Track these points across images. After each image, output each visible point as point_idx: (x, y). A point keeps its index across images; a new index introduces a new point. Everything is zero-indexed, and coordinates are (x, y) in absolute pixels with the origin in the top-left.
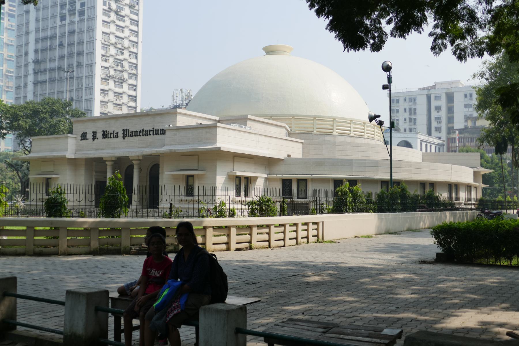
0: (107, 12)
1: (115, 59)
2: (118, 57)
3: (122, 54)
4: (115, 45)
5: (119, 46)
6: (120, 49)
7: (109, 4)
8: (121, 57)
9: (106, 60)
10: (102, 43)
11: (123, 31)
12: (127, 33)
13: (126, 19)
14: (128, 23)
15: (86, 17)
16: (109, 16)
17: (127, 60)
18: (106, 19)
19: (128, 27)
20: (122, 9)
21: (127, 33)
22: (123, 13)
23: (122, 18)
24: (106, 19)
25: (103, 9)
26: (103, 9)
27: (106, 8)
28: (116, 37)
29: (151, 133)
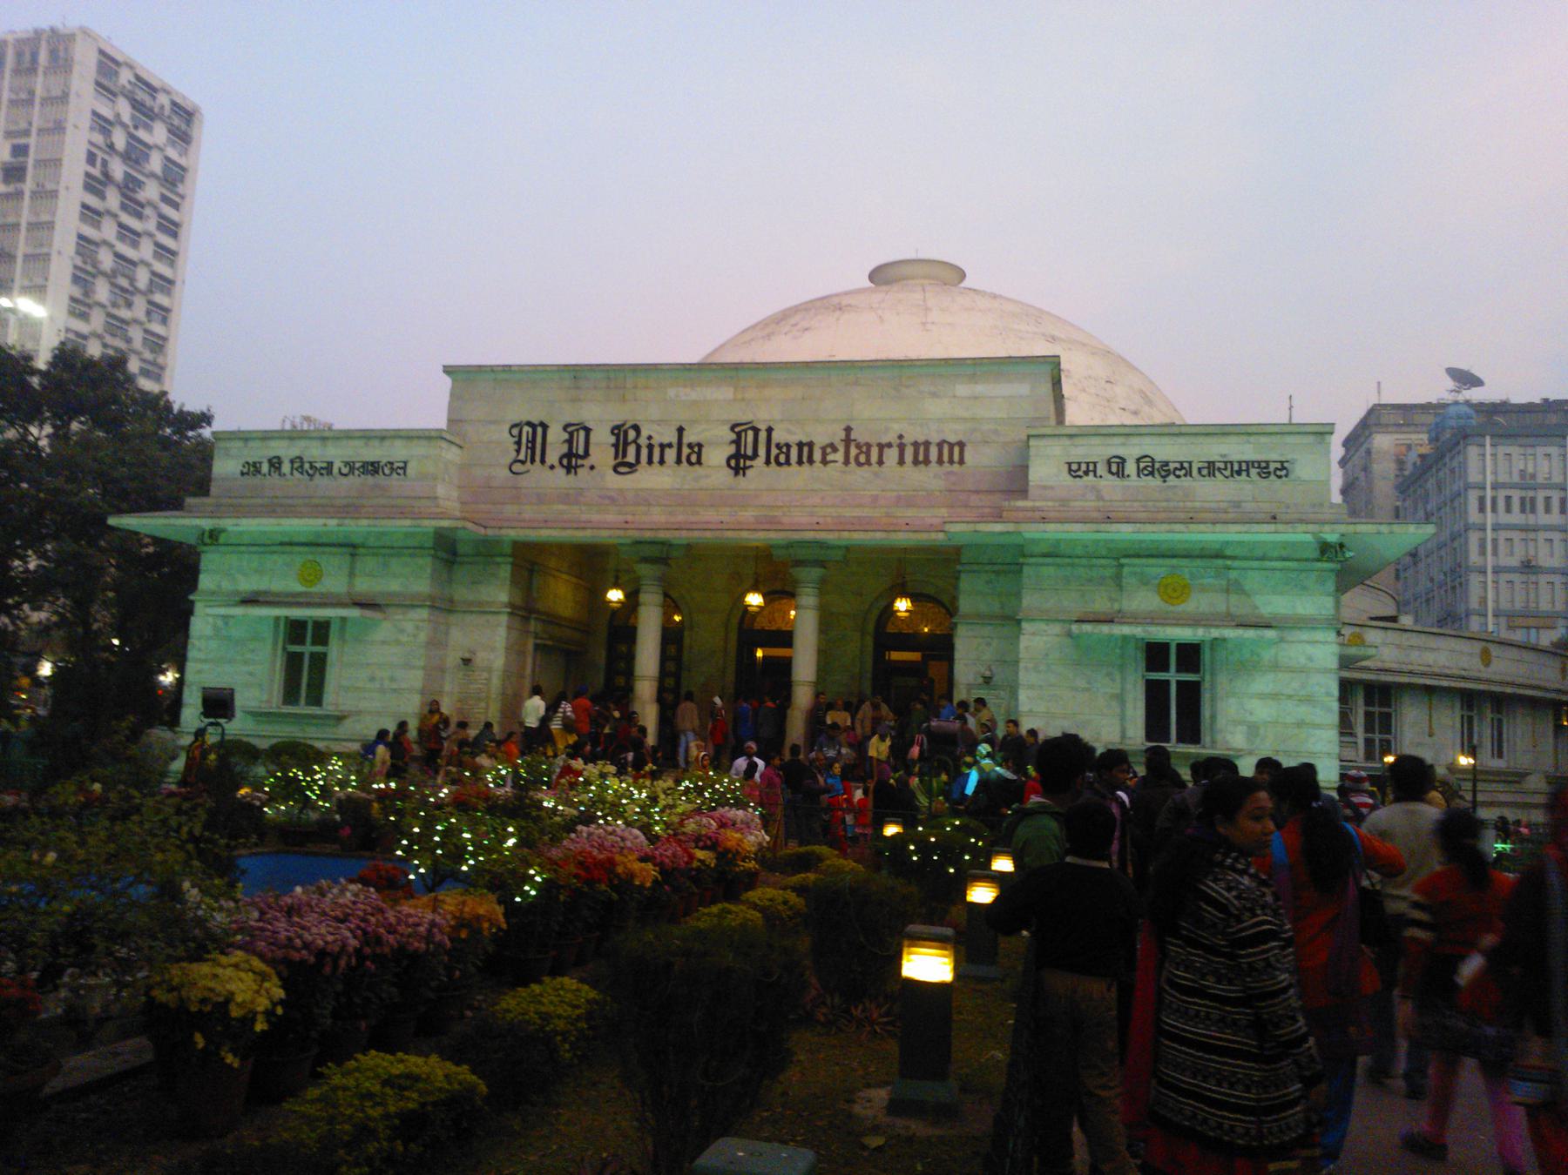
0: (95, 185)
1: (109, 315)
2: (115, 311)
3: (129, 305)
4: (110, 276)
5: (124, 282)
6: (123, 290)
7: (105, 163)
8: (124, 313)
9: (84, 316)
10: (76, 267)
11: (135, 245)
12: (146, 250)
13: (148, 211)
14: (151, 225)
15: (28, 186)
16: (102, 197)
17: (141, 323)
18: (93, 201)
19: (151, 235)
20: (140, 184)
21: (146, 250)
22: (142, 196)
23: (134, 206)
24: (93, 201)
25: (88, 175)
26: (88, 175)
27: (96, 172)
28: (118, 256)
29: (891, 455)
